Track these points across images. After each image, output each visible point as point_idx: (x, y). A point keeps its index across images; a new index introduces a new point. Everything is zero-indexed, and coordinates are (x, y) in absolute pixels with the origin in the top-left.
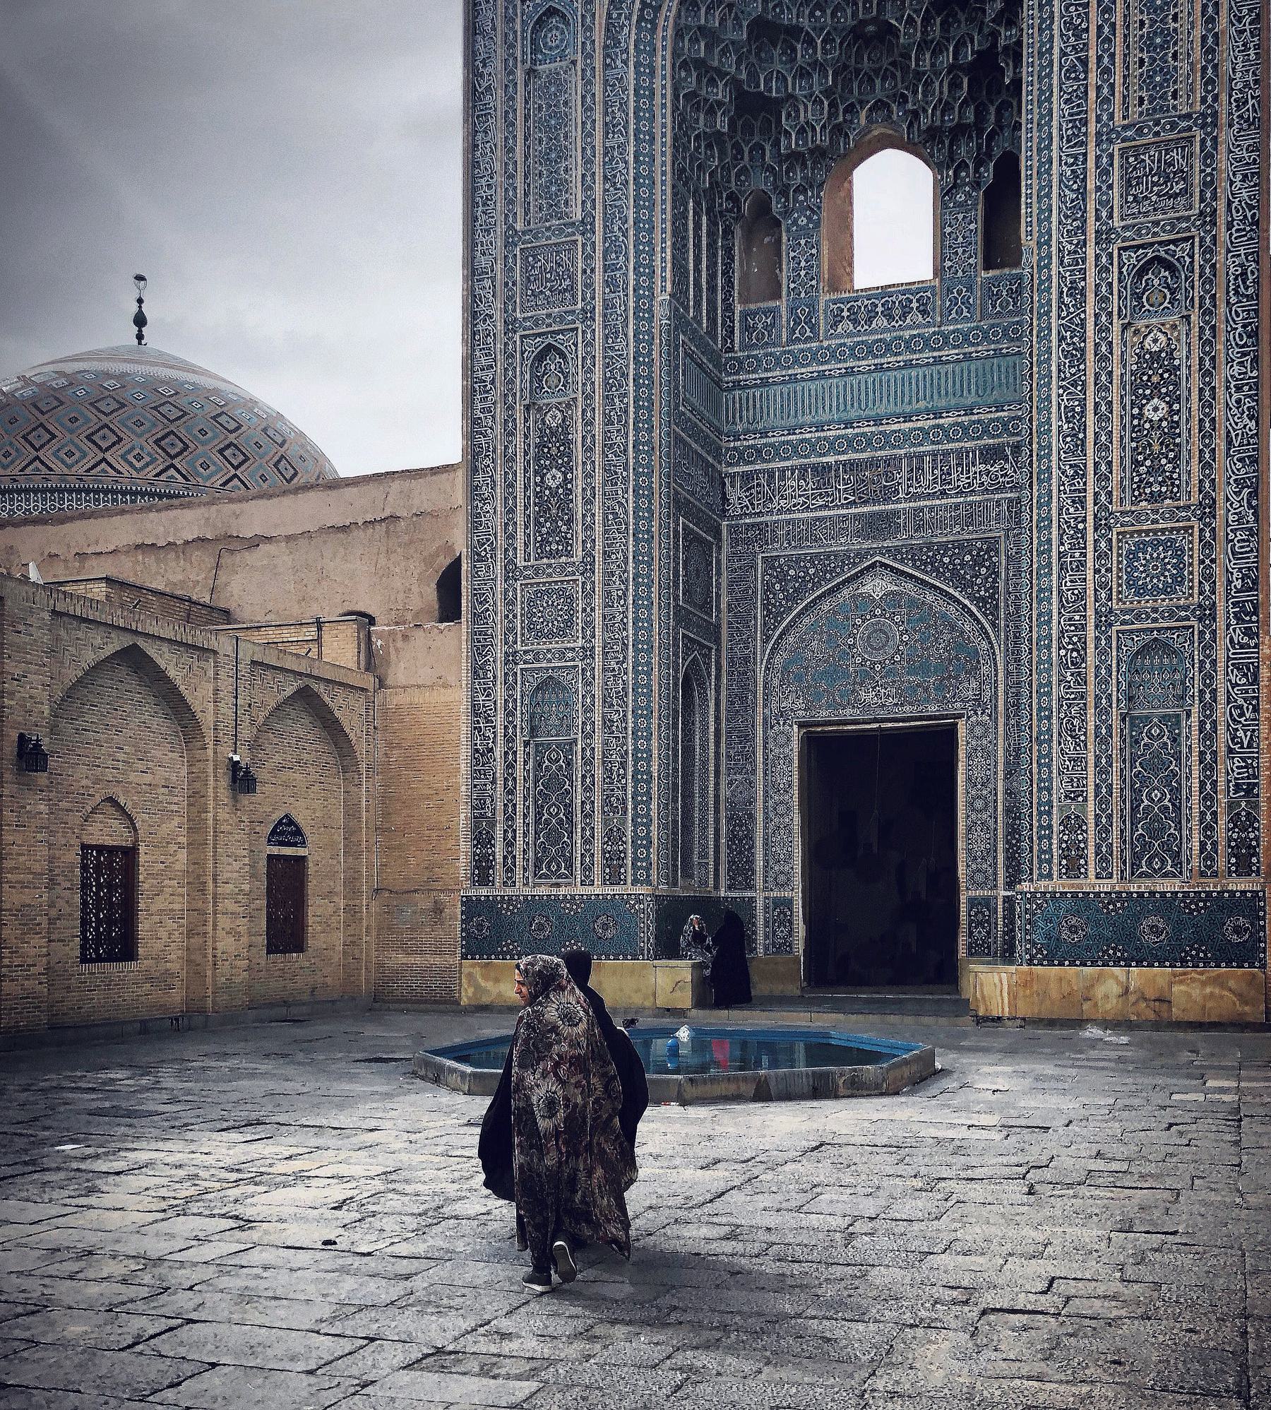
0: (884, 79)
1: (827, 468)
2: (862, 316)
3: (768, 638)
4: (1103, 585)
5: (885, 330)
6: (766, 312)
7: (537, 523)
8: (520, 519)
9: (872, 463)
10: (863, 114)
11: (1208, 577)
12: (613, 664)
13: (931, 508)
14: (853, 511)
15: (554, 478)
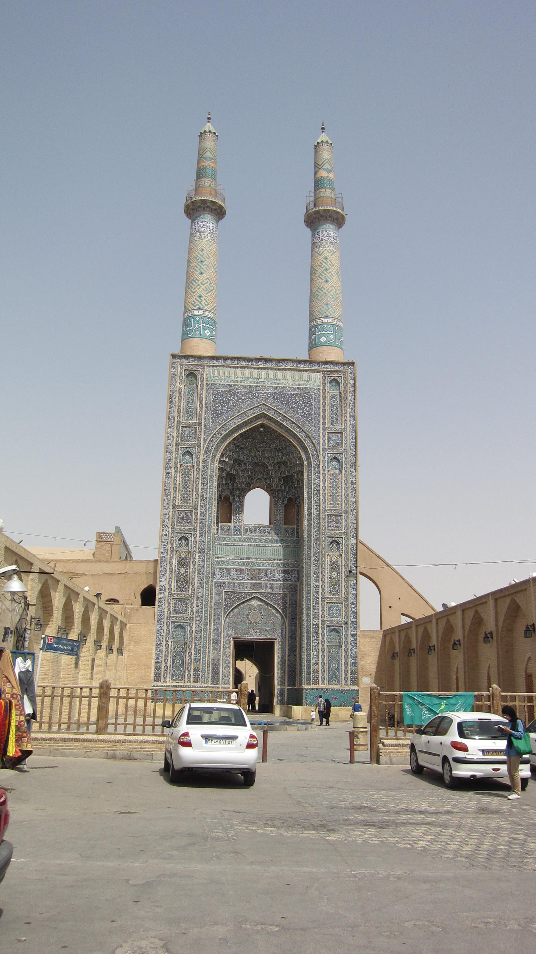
0: (261, 473)
1: (243, 569)
2: (253, 531)
3: (225, 613)
4: (323, 614)
5: (259, 536)
6: (227, 526)
7: (177, 582)
8: (173, 581)
9: (254, 570)
10: (255, 480)
11: (346, 615)
12: (198, 622)
13: (270, 584)
14: (250, 582)
15: (183, 571)
